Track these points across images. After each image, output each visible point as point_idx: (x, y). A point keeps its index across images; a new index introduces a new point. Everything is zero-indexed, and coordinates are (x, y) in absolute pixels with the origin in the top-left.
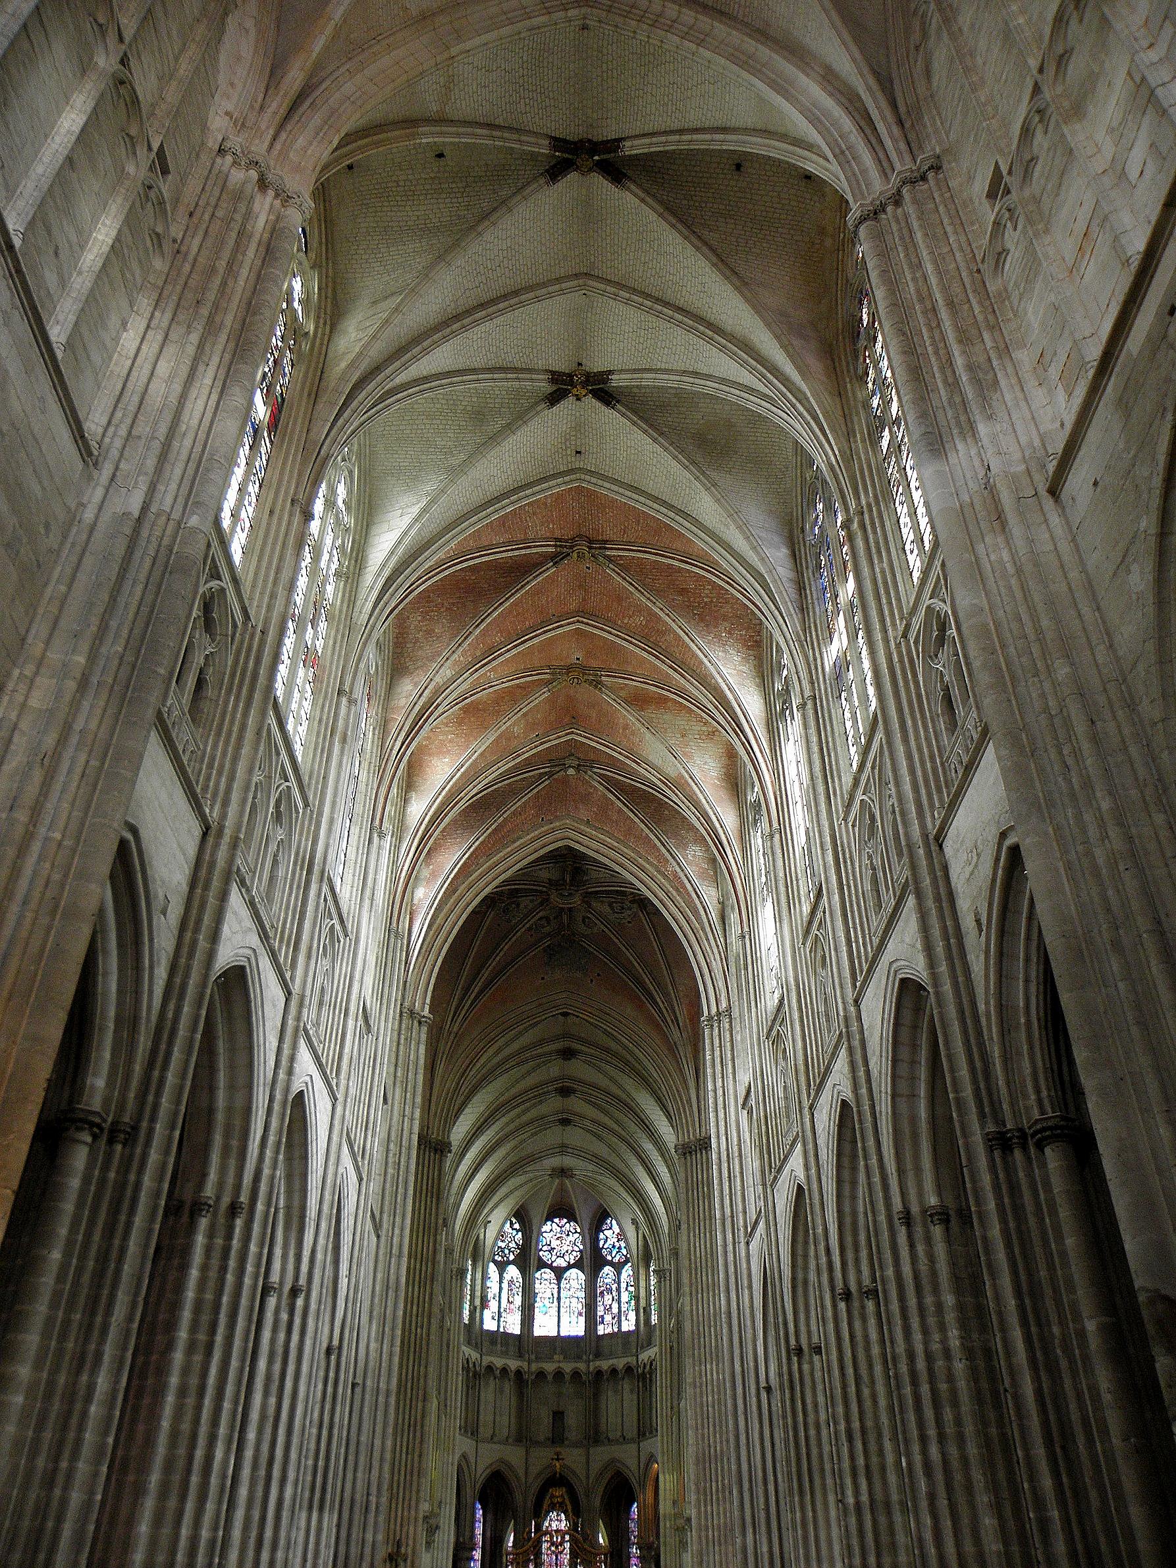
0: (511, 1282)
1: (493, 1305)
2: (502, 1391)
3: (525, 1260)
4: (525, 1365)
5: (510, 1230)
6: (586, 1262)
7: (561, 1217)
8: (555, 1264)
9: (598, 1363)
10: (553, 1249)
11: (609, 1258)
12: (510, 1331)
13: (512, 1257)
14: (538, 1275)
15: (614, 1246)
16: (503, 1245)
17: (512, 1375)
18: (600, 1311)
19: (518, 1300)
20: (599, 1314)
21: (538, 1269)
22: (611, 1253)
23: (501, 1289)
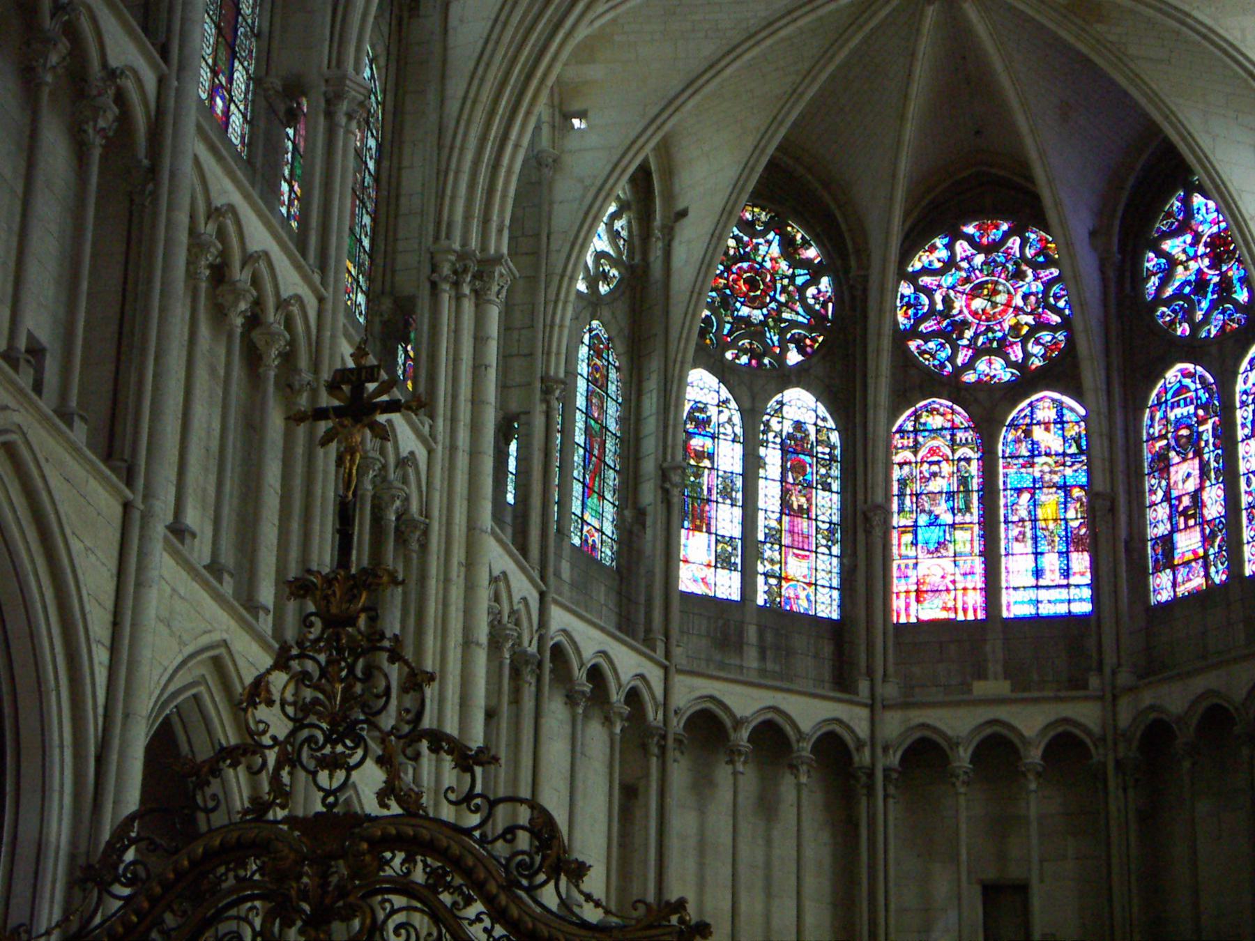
0: (794, 446)
1: (727, 519)
2: (767, 806)
4: (857, 719)
5: (783, 265)
6: (1089, 348)
7: (985, 212)
8: (970, 377)
9: (1147, 698)
10: (965, 324)
11: (1183, 329)
12: (802, 606)
13: (793, 357)
14: (904, 419)
15: (1200, 283)
16: (757, 315)
17: (805, 749)
18: (1158, 519)
19: (828, 505)
20: (1152, 532)
21: (902, 399)
22: (1188, 315)
23: (752, 463)
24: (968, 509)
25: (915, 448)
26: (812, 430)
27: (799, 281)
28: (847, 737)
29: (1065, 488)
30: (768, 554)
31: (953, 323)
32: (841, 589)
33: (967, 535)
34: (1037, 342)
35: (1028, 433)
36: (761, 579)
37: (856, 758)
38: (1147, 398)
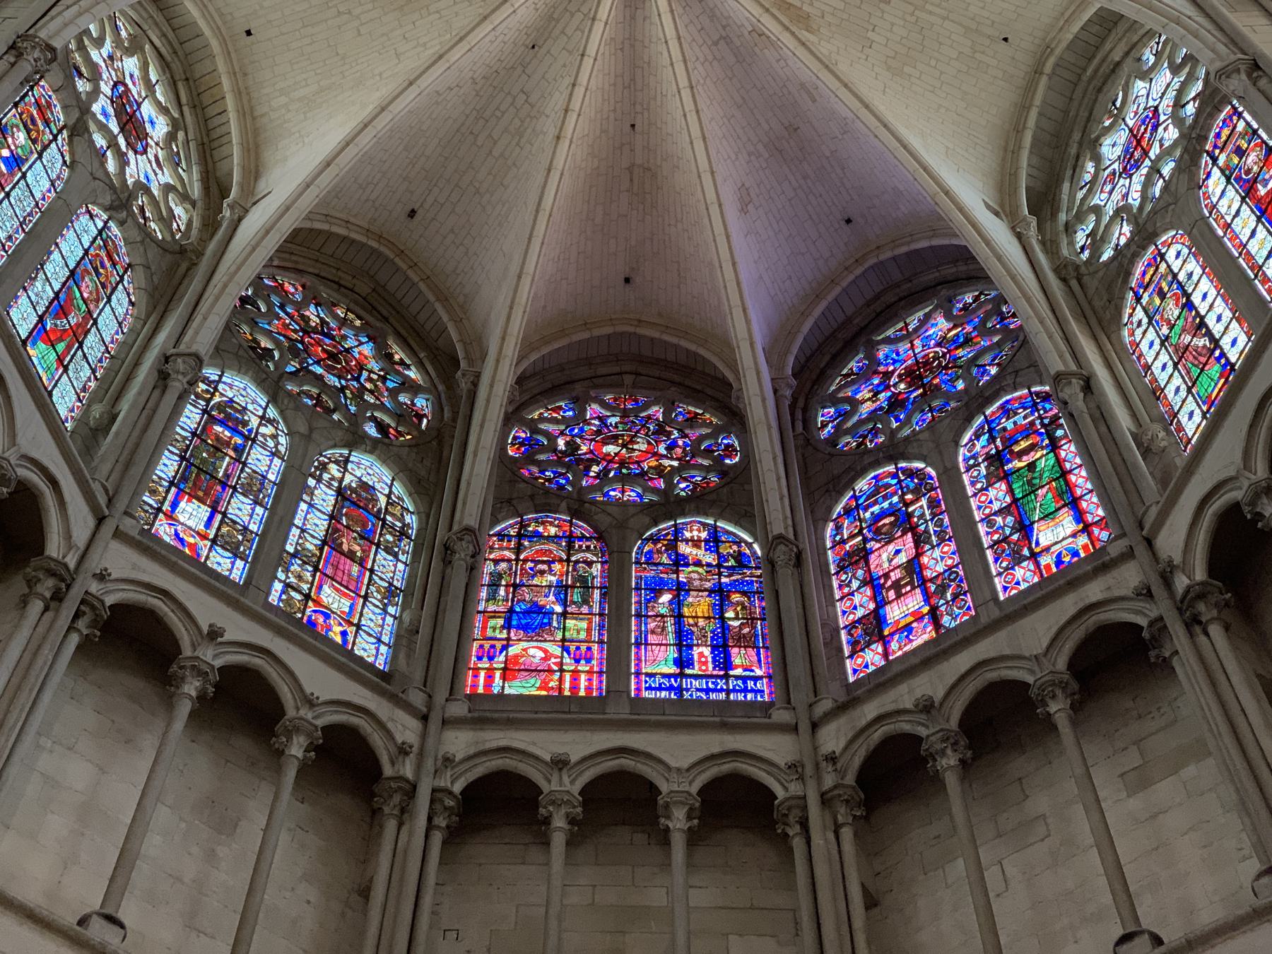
3: (441, 465)
14: (508, 525)
24: (586, 601)
25: (518, 549)
26: (383, 501)
27: (390, 385)
28: (377, 740)
29: (721, 594)
30: (295, 568)
31: (579, 461)
32: (395, 647)
33: (584, 625)
34: (685, 479)
35: (672, 546)
36: (278, 586)
37: (388, 771)
38: (830, 510)
